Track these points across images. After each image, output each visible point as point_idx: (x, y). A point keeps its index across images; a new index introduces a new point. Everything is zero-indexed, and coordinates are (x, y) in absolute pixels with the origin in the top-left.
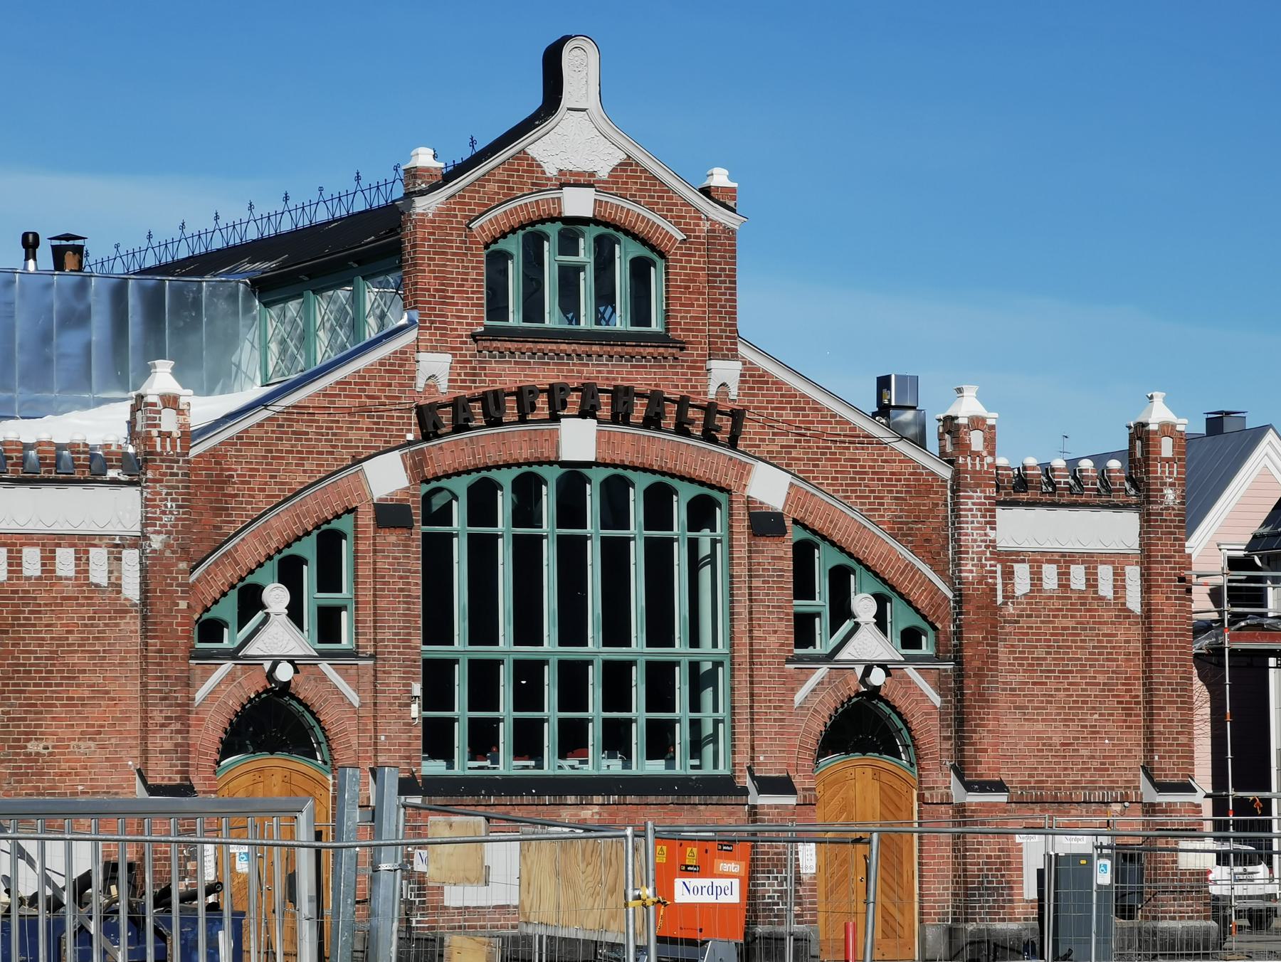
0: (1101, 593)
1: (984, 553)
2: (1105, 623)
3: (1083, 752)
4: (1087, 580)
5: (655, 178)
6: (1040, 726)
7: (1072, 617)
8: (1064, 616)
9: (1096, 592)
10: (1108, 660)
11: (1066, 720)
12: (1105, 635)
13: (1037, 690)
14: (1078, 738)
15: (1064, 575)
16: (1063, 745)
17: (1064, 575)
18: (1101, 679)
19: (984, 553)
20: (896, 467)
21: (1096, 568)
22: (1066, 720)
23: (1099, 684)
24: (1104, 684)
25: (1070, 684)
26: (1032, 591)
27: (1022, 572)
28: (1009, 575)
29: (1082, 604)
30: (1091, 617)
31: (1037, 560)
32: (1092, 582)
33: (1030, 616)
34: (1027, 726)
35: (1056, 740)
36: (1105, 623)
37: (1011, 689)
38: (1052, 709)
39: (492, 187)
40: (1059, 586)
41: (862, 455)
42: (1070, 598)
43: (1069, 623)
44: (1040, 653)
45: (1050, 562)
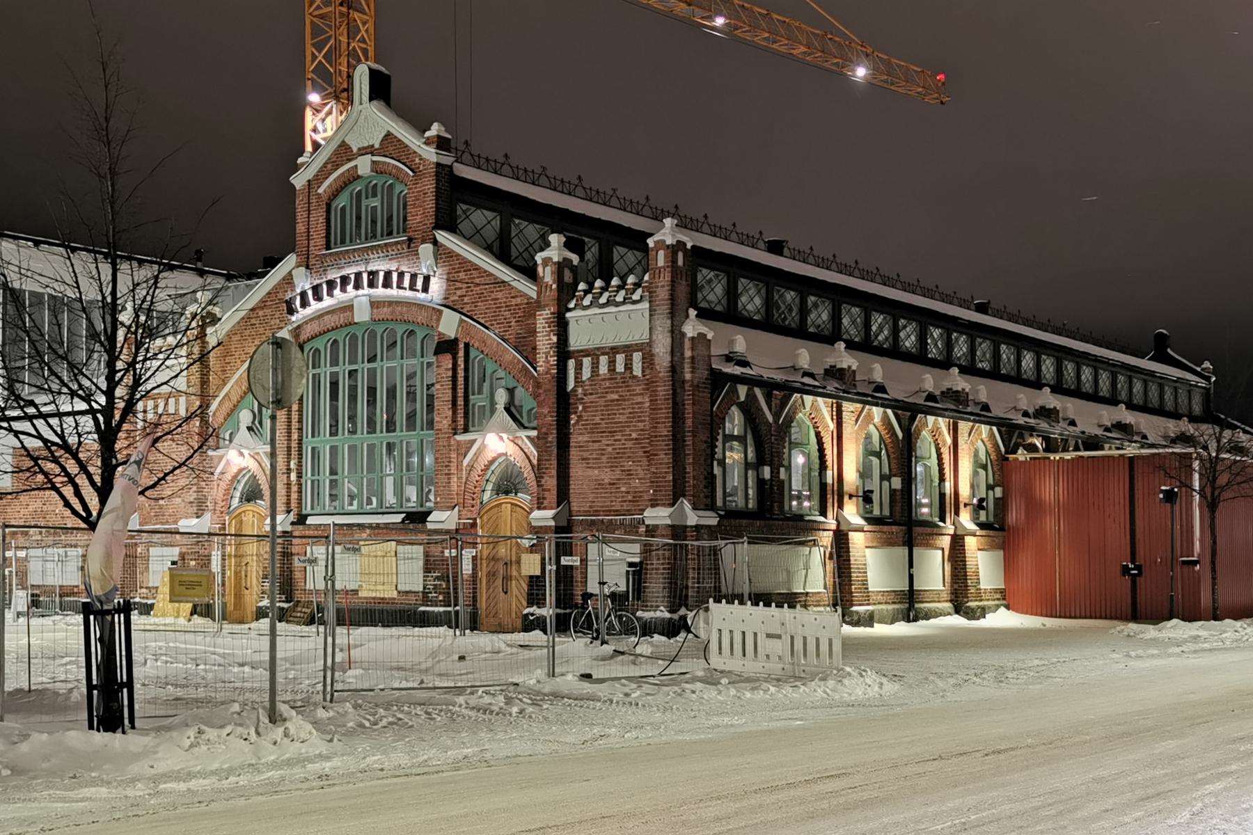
0: (635, 373)
1: (549, 352)
2: (637, 395)
3: (623, 489)
4: (626, 365)
5: (399, 140)
6: (596, 472)
7: (617, 392)
8: (612, 392)
9: (631, 373)
10: (639, 421)
11: (612, 467)
12: (637, 403)
13: (596, 445)
14: (619, 479)
15: (612, 363)
16: (610, 484)
17: (612, 363)
18: (634, 435)
19: (549, 352)
20: (519, 300)
21: (631, 355)
22: (612, 467)
23: (632, 439)
24: (636, 439)
25: (615, 440)
26: (592, 376)
27: (587, 361)
28: (579, 367)
29: (623, 382)
30: (629, 391)
31: (594, 354)
32: (628, 366)
33: (591, 394)
34: (589, 472)
35: (607, 481)
36: (637, 395)
37: (580, 447)
38: (604, 459)
39: (329, 166)
40: (609, 370)
41: (500, 295)
42: (616, 379)
43: (615, 396)
44: (597, 420)
45: (604, 354)
